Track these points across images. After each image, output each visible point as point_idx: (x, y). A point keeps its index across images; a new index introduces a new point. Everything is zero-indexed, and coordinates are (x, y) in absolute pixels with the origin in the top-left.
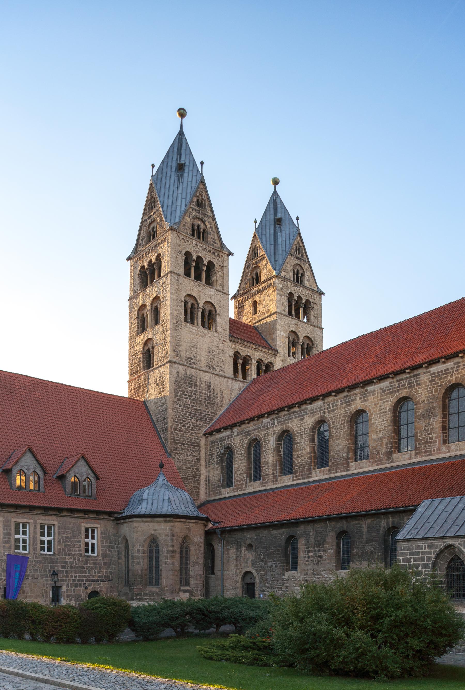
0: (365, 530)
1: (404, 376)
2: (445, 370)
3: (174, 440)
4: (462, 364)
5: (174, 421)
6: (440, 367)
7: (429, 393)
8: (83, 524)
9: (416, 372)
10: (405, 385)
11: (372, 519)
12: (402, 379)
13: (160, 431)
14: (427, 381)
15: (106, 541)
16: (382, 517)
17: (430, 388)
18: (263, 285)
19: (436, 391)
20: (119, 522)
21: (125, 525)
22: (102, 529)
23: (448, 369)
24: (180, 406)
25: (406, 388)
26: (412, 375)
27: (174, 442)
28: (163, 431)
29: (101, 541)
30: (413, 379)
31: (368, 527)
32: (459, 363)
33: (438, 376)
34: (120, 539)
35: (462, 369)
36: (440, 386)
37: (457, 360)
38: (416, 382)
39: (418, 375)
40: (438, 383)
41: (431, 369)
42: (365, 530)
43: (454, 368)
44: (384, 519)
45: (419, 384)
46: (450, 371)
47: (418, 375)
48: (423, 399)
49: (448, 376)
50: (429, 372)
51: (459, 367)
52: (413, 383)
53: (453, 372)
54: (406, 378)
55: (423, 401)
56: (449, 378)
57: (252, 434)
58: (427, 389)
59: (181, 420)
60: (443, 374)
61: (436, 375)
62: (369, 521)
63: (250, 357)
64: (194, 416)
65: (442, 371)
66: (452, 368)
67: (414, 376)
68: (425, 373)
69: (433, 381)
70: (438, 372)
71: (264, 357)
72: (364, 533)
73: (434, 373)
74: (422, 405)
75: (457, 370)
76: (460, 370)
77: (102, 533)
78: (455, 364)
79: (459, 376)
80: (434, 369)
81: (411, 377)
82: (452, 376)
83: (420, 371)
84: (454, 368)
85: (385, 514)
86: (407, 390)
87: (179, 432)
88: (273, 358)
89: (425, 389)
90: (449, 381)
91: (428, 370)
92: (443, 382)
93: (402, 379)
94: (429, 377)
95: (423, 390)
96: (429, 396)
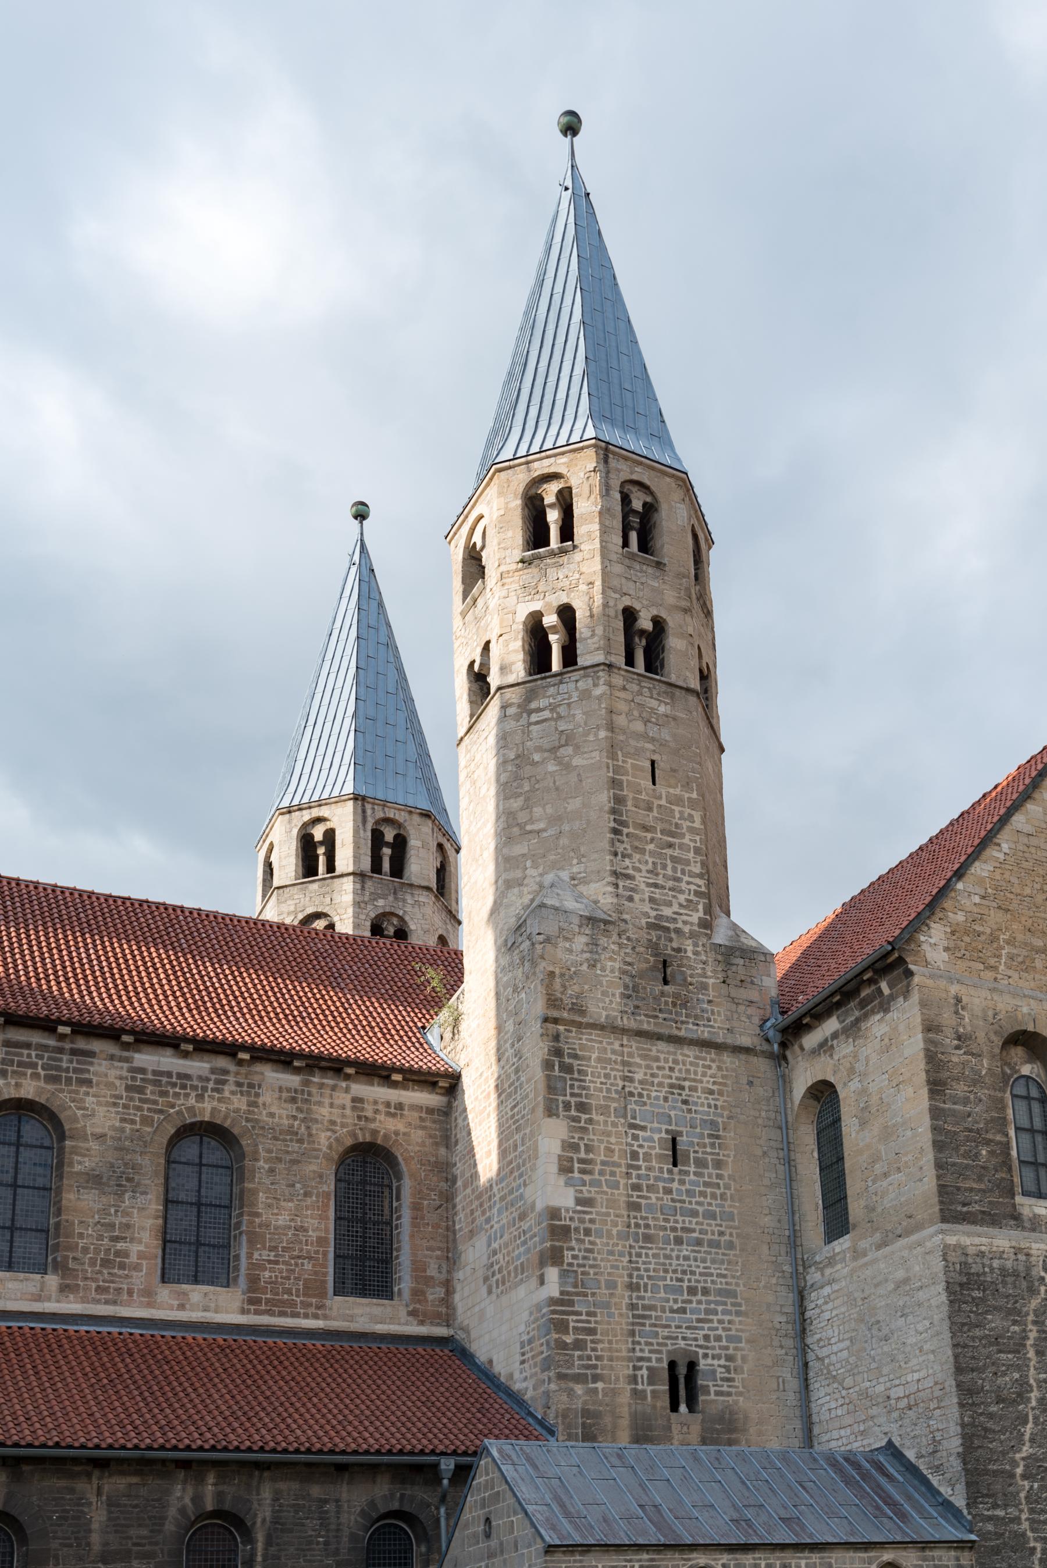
0: (98, 1516)
1: (36, 1038)
2: (180, 1076)
4: (231, 1079)
6: (166, 1061)
7: (123, 1120)
9: (81, 1044)
10: (34, 1066)
11: (134, 1480)
12: (28, 1046)
14: (118, 1083)
16: (181, 1474)
17: (125, 1106)
19: (145, 1120)
23: (188, 1077)
25: (36, 1076)
26: (68, 1046)
30: (65, 1057)
31: (111, 1504)
32: (226, 1072)
33: (157, 1083)
35: (233, 1093)
36: (161, 1112)
37: (222, 1062)
38: (75, 1070)
39: (92, 1054)
40: (155, 1102)
41: (137, 1056)
42: (98, 1516)
43: (208, 1080)
44: (185, 1482)
45: (89, 1082)
46: (195, 1083)
47: (92, 1054)
48: (98, 1131)
49: (187, 1095)
50: (127, 1060)
51: (224, 1082)
52: (67, 1070)
53: (205, 1089)
54: (45, 1048)
55: (100, 1137)
56: (192, 1101)
58: (115, 1104)
60: (174, 1085)
61: (150, 1077)
62: (117, 1484)
65: (169, 1074)
66: (200, 1078)
67: (74, 1052)
68: (112, 1058)
69: (141, 1090)
70: (155, 1073)
72: (95, 1526)
73: (142, 1071)
74: (94, 1145)
75: (217, 1090)
76: (227, 1094)
78: (213, 1071)
79: (223, 1107)
80: (147, 1059)
81: (61, 1050)
82: (200, 1098)
83: (97, 1046)
84: (208, 1080)
85: (190, 1465)
86: (42, 1084)
89: (107, 1104)
90: (191, 1110)
91: (126, 1054)
92: (173, 1106)
93: (28, 1046)
94: (125, 1073)
95: (99, 1103)
96: (122, 1130)
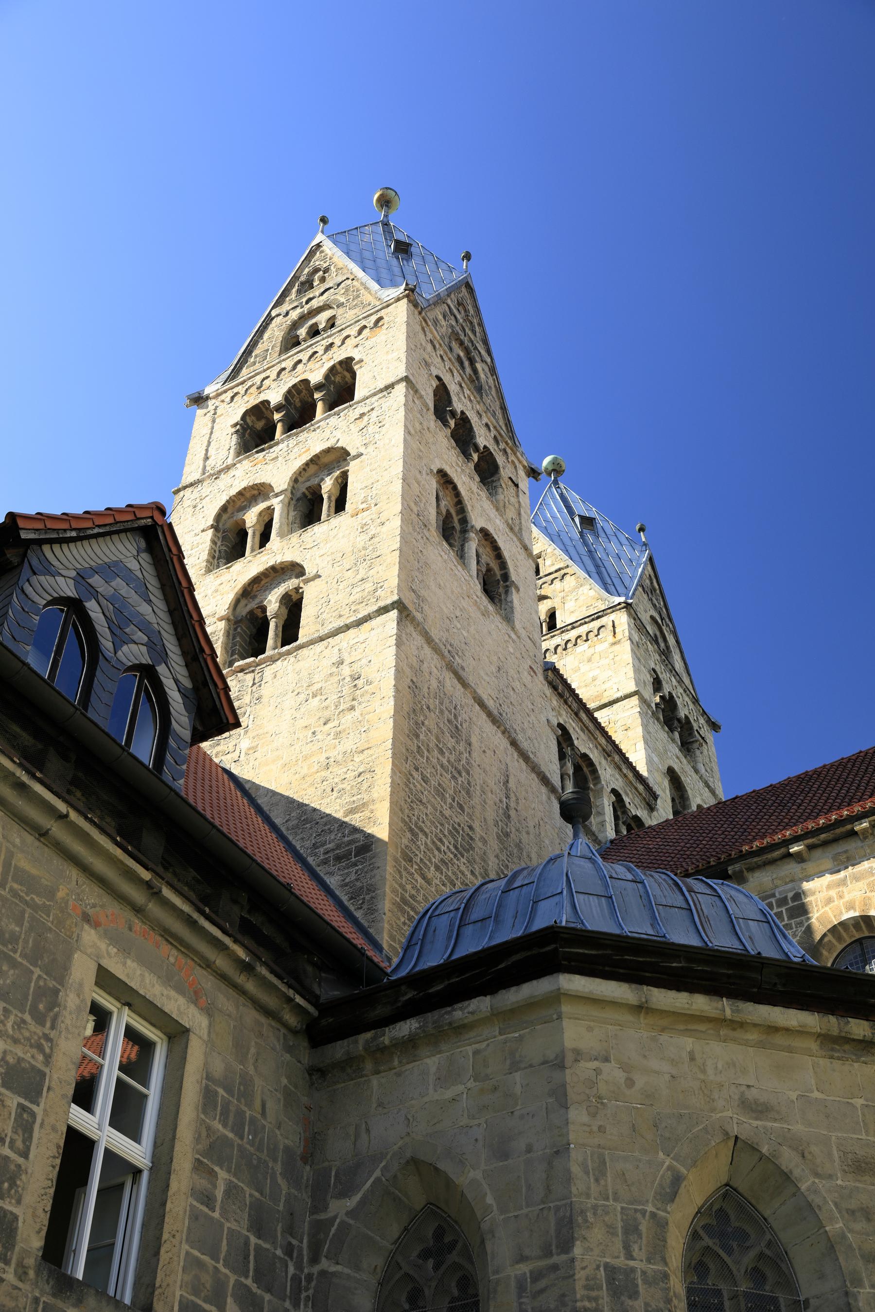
3: (404, 900)
5: (403, 821)
8: (89, 936)
13: (325, 862)
15: (231, 1191)
18: (566, 636)
20: (339, 1050)
21: (432, 1063)
22: (218, 1068)
24: (425, 780)
27: (403, 912)
28: (338, 859)
29: (198, 1166)
34: (339, 1208)
57: (829, 900)
59: (426, 835)
63: (594, 771)
64: (468, 851)
71: (627, 795)
77: (208, 1098)
87: (419, 879)
88: (646, 812)
